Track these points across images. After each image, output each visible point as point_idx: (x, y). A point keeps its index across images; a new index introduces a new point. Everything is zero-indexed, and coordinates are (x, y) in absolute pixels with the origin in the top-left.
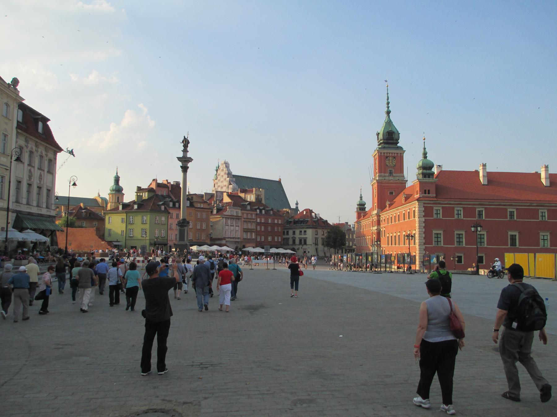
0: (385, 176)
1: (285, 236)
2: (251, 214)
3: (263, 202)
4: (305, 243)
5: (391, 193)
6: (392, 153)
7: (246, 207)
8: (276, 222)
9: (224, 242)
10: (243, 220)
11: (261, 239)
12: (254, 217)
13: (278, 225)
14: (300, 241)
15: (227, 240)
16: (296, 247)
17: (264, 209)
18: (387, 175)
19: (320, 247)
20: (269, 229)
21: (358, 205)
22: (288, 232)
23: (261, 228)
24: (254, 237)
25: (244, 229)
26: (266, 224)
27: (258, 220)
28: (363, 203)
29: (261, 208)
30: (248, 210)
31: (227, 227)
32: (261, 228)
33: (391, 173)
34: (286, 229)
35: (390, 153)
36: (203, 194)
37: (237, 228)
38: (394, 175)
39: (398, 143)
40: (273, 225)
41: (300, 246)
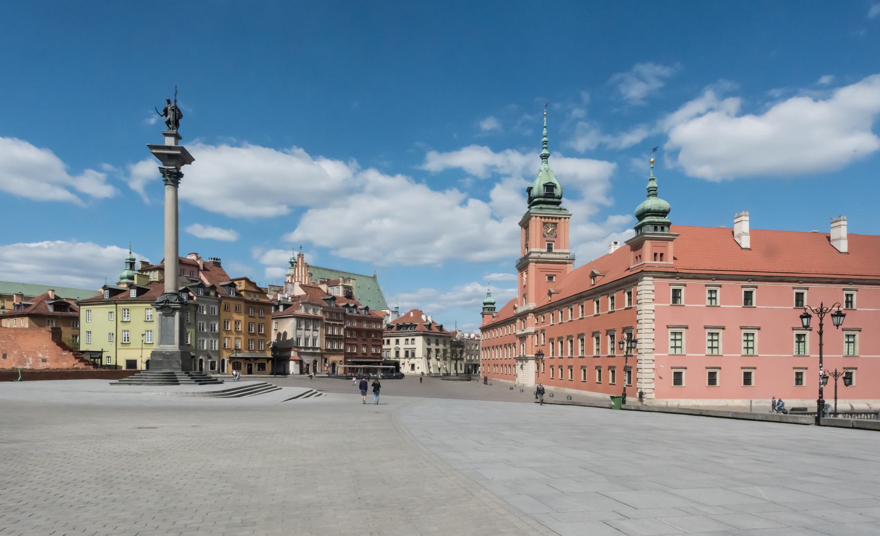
0: (542, 253)
4: (413, 355)
5: (550, 278)
6: (552, 218)
12: (341, 317)
14: (407, 352)
18: (545, 250)
19: (433, 361)
21: (485, 304)
28: (492, 301)
29: (352, 305)
33: (550, 249)
35: (549, 218)
37: (316, 334)
38: (554, 250)
39: (558, 204)
41: (407, 360)
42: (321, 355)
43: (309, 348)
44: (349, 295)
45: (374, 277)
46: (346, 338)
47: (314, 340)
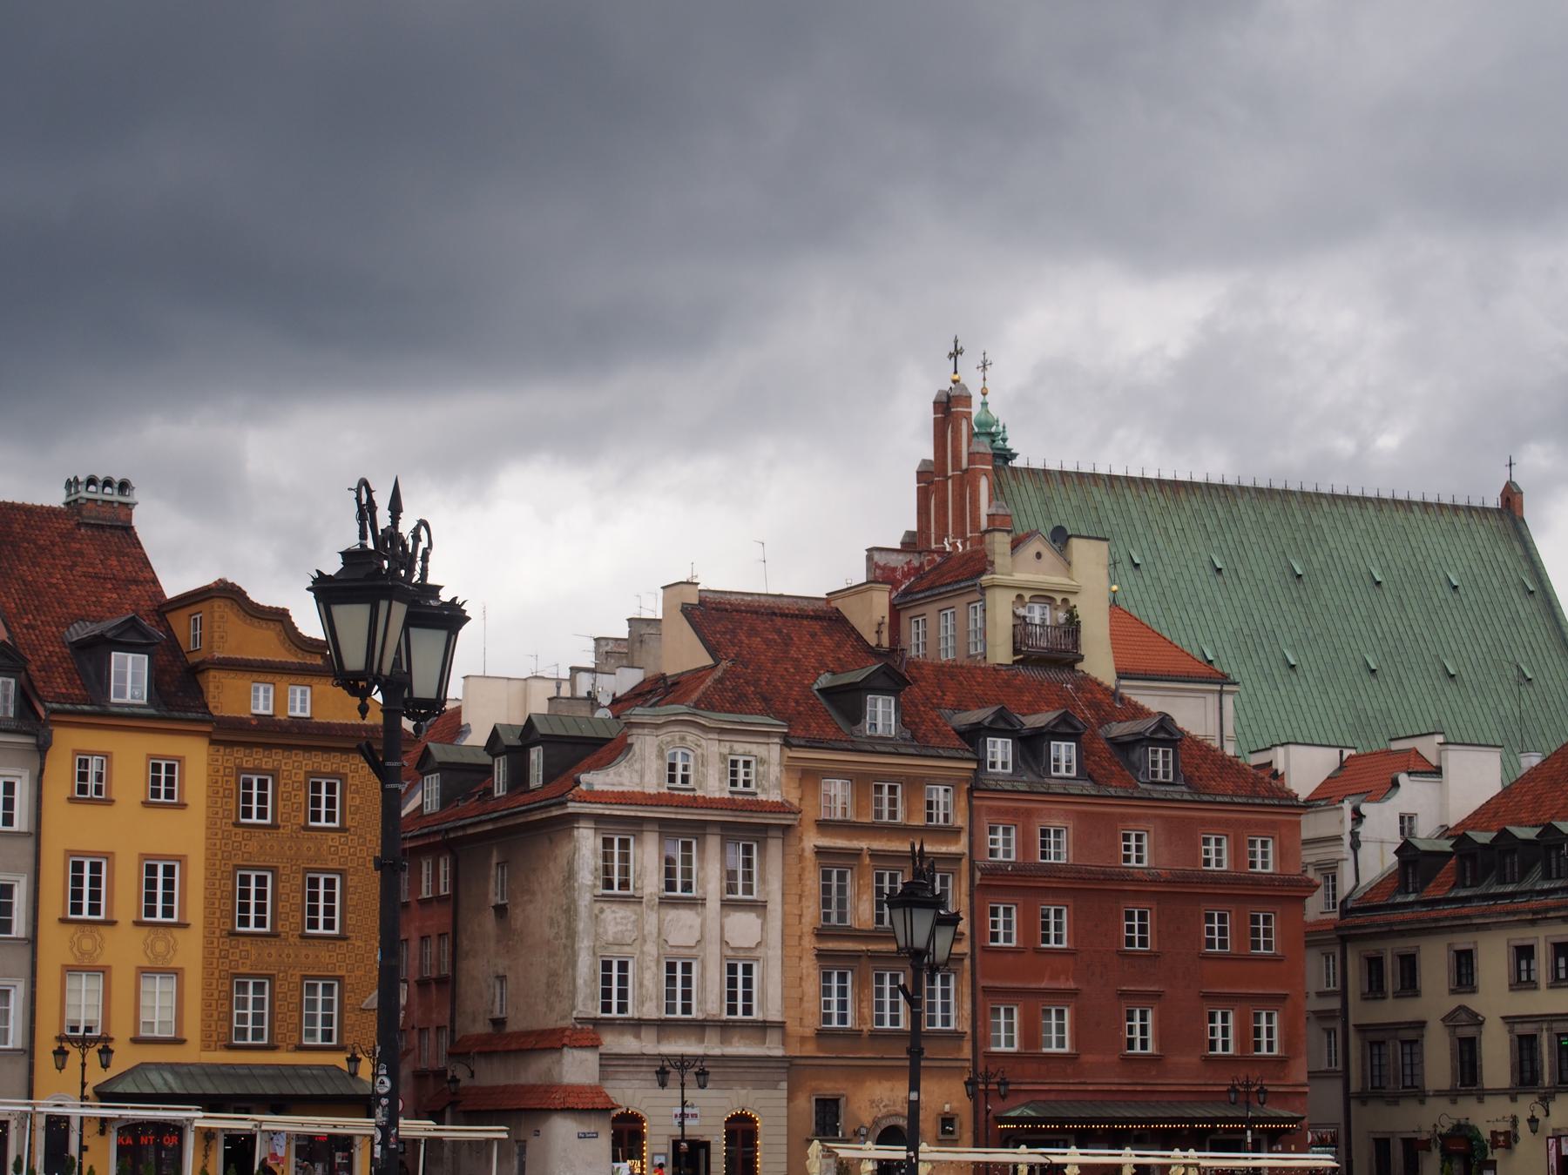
1: (1391, 1011)
2: (915, 784)
3: (1099, 662)
7: (855, 715)
8: (1218, 856)
9: (577, 1068)
10: (812, 840)
11: (1032, 1034)
13: (1243, 891)
14: (1525, 1046)
15: (628, 1044)
16: (1487, 1117)
17: (1066, 729)
20: (1141, 929)
22: (1409, 964)
23: (1036, 927)
24: (960, 1020)
25: (821, 934)
26: (1093, 888)
27: (1003, 847)
30: (876, 745)
31: (616, 920)
32: (1036, 927)
34: (1391, 933)
36: (623, 632)
37: (744, 929)
40: (1185, 891)
41: (1525, 1107)
42: (791, 1069)
43: (700, 1027)
44: (1051, 655)
45: (1511, 497)
46: (983, 952)
47: (738, 973)
